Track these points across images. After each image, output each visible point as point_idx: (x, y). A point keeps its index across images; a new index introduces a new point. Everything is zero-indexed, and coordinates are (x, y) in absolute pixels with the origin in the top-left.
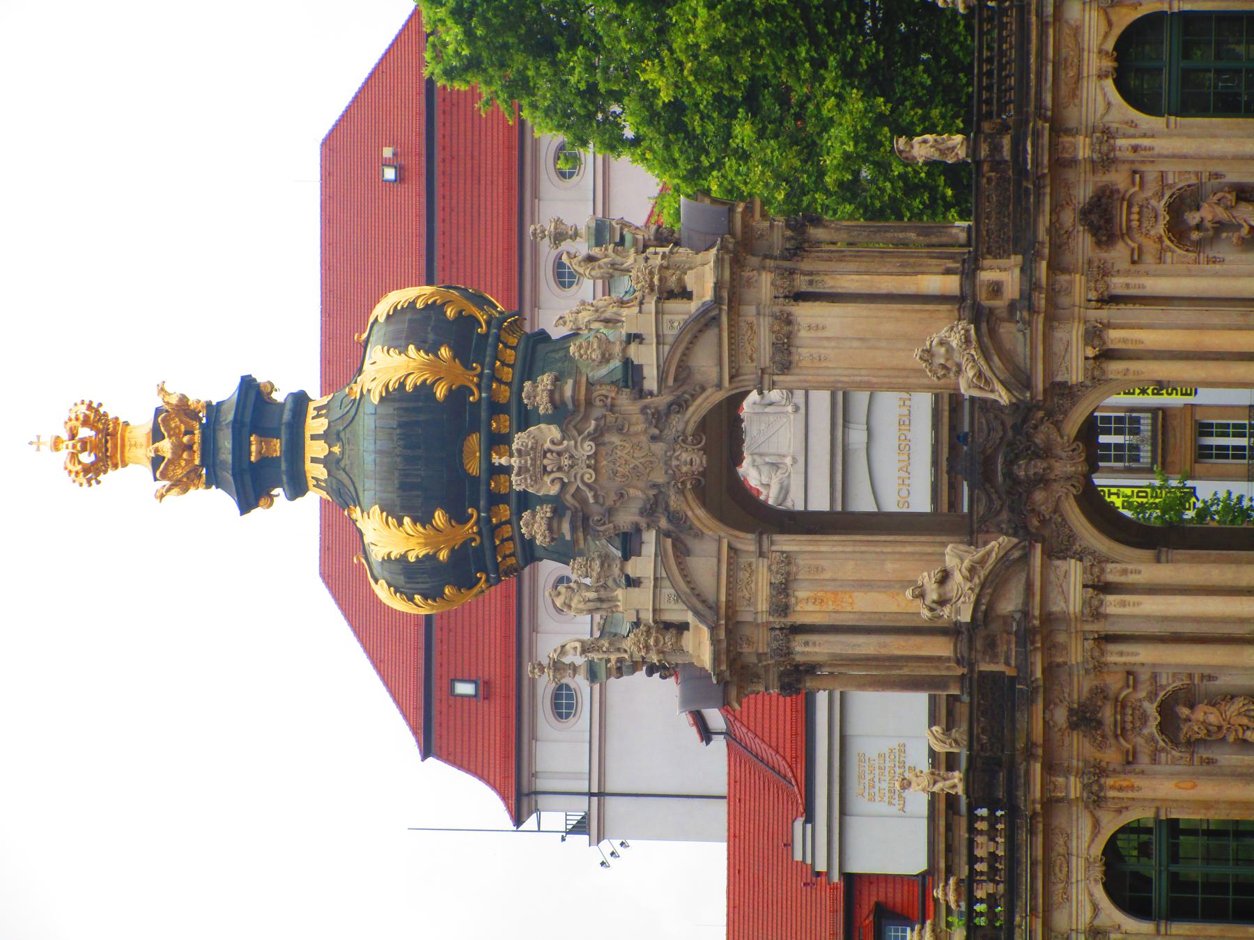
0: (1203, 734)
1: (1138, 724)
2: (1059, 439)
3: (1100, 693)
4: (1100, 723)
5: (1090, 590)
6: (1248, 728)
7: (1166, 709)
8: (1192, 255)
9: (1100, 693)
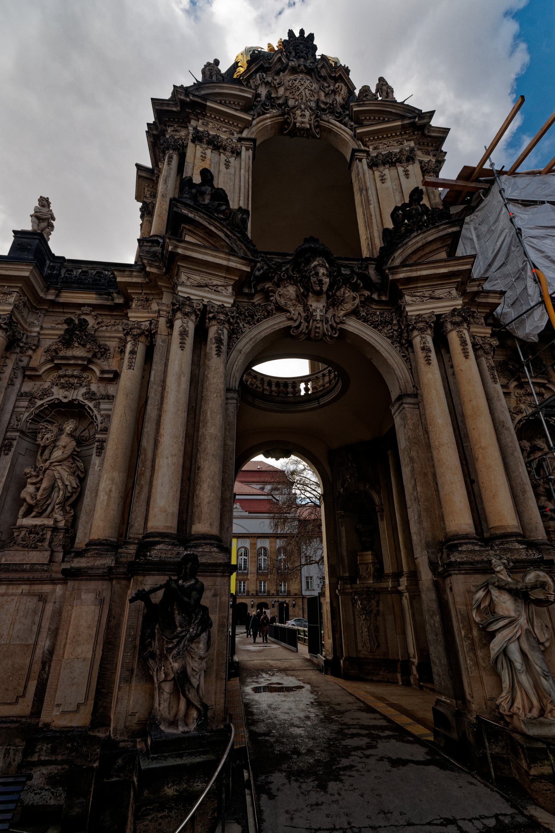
1: (62, 381)
2: (342, 313)
6: (38, 489)
7: (75, 411)
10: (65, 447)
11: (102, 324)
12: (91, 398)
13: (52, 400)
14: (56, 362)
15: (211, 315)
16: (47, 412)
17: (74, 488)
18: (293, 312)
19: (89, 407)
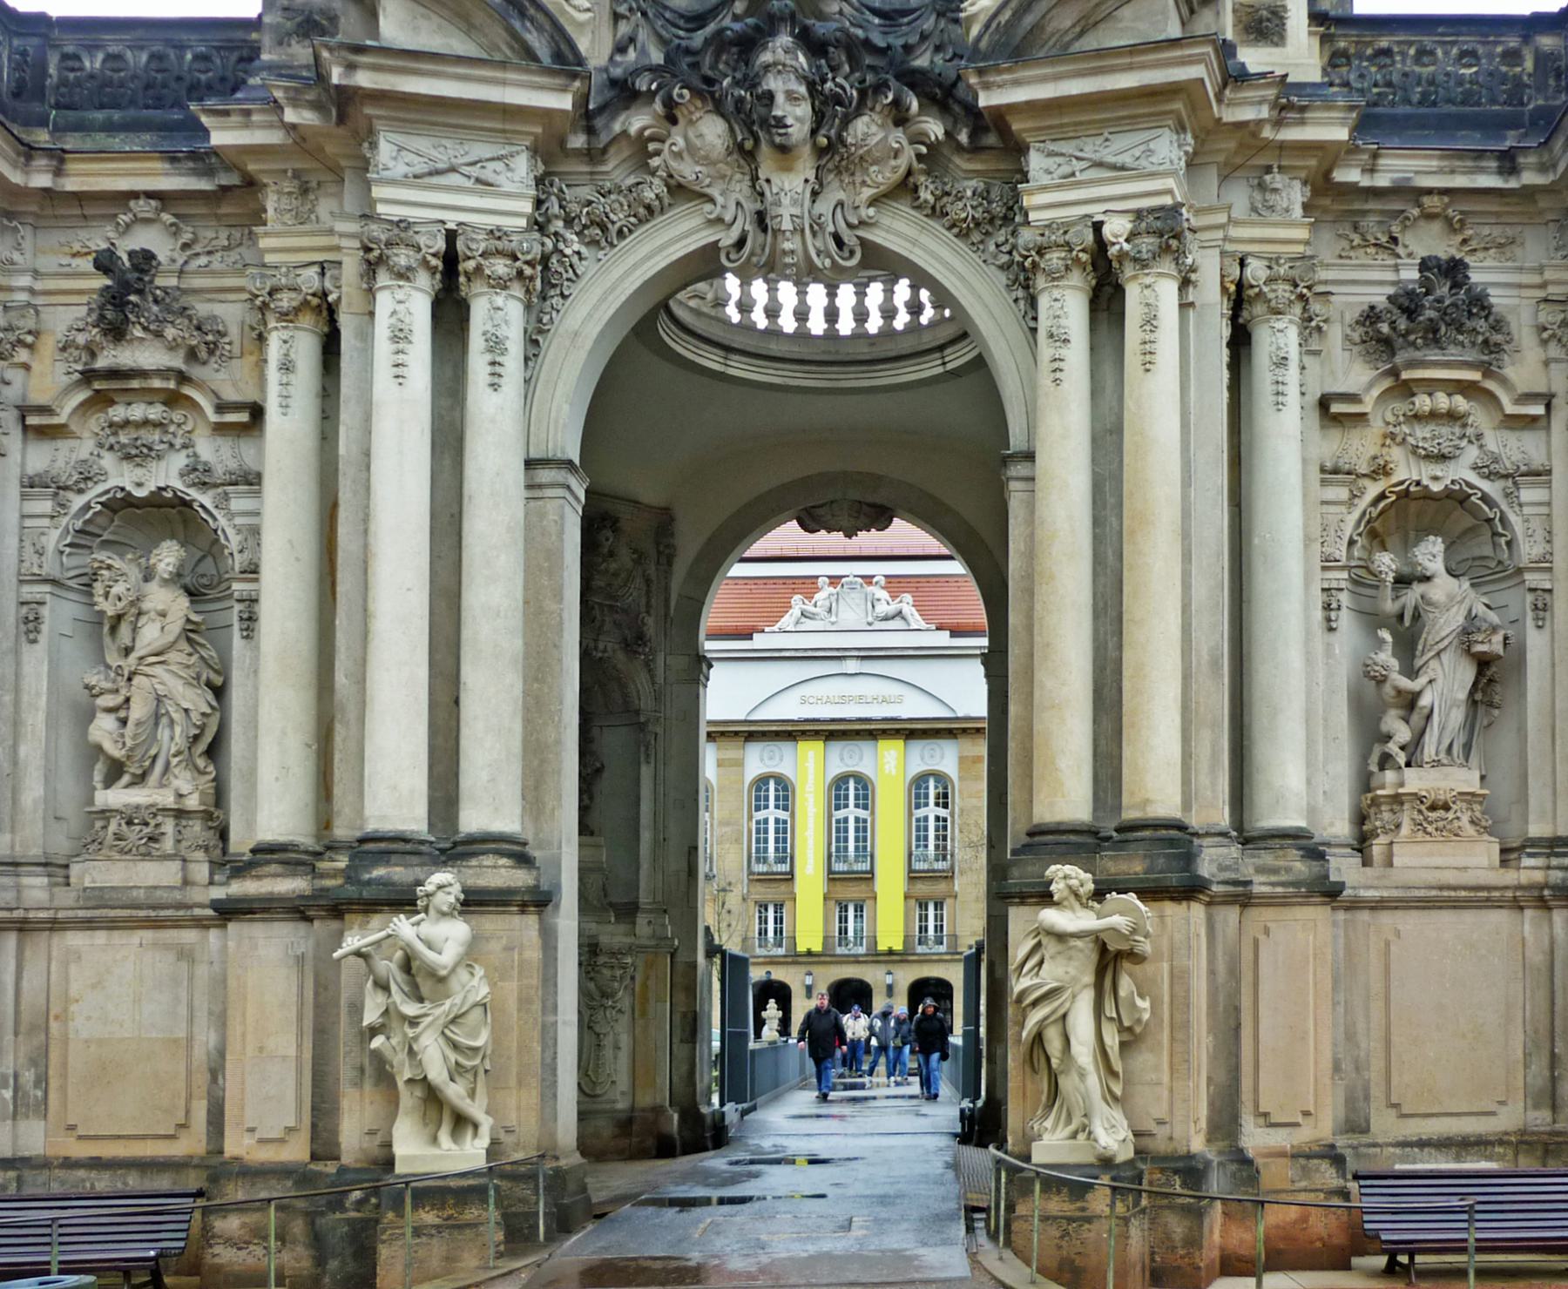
0: (110, 609)
2: (867, 193)
3: (207, 344)
4: (117, 333)
5: (441, 245)
6: (124, 722)
7: (168, 514)
8: (1341, 552)
9: (207, 344)
10: (163, 615)
11: (198, 248)
12: (205, 484)
13: (107, 492)
14: (97, 386)
15: (471, 265)
16: (101, 520)
17: (203, 714)
18: (720, 200)
19: (202, 506)
